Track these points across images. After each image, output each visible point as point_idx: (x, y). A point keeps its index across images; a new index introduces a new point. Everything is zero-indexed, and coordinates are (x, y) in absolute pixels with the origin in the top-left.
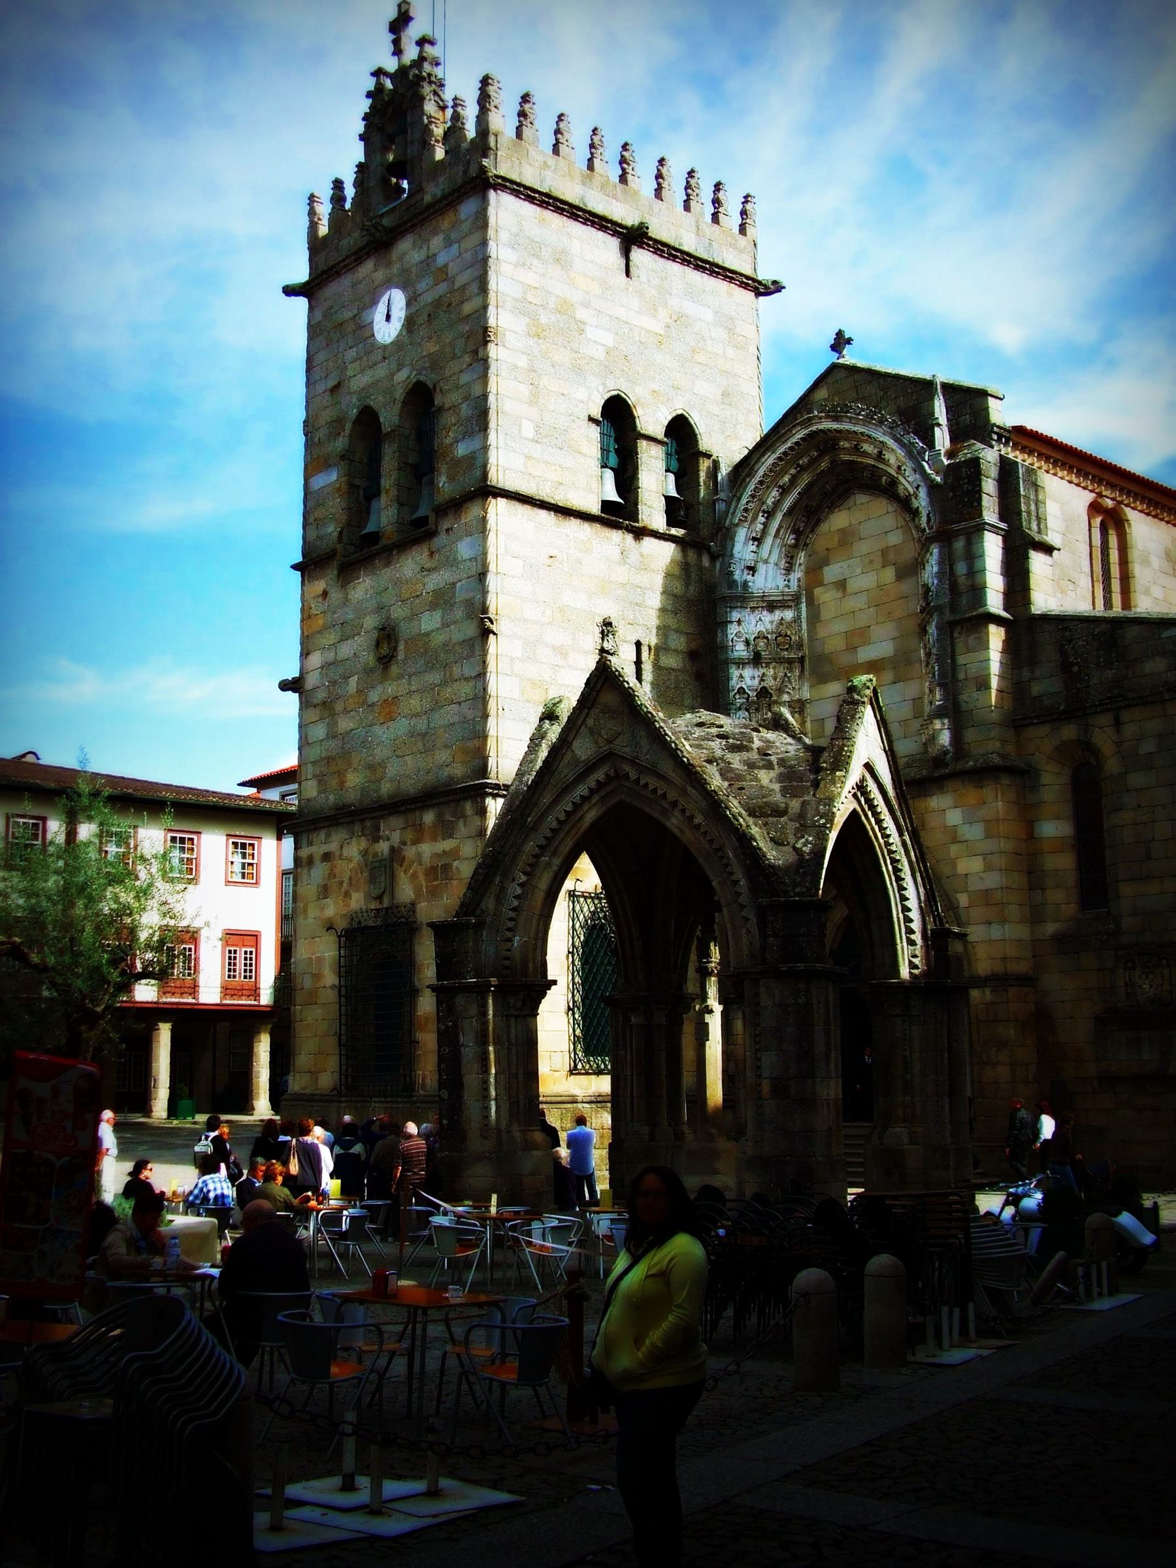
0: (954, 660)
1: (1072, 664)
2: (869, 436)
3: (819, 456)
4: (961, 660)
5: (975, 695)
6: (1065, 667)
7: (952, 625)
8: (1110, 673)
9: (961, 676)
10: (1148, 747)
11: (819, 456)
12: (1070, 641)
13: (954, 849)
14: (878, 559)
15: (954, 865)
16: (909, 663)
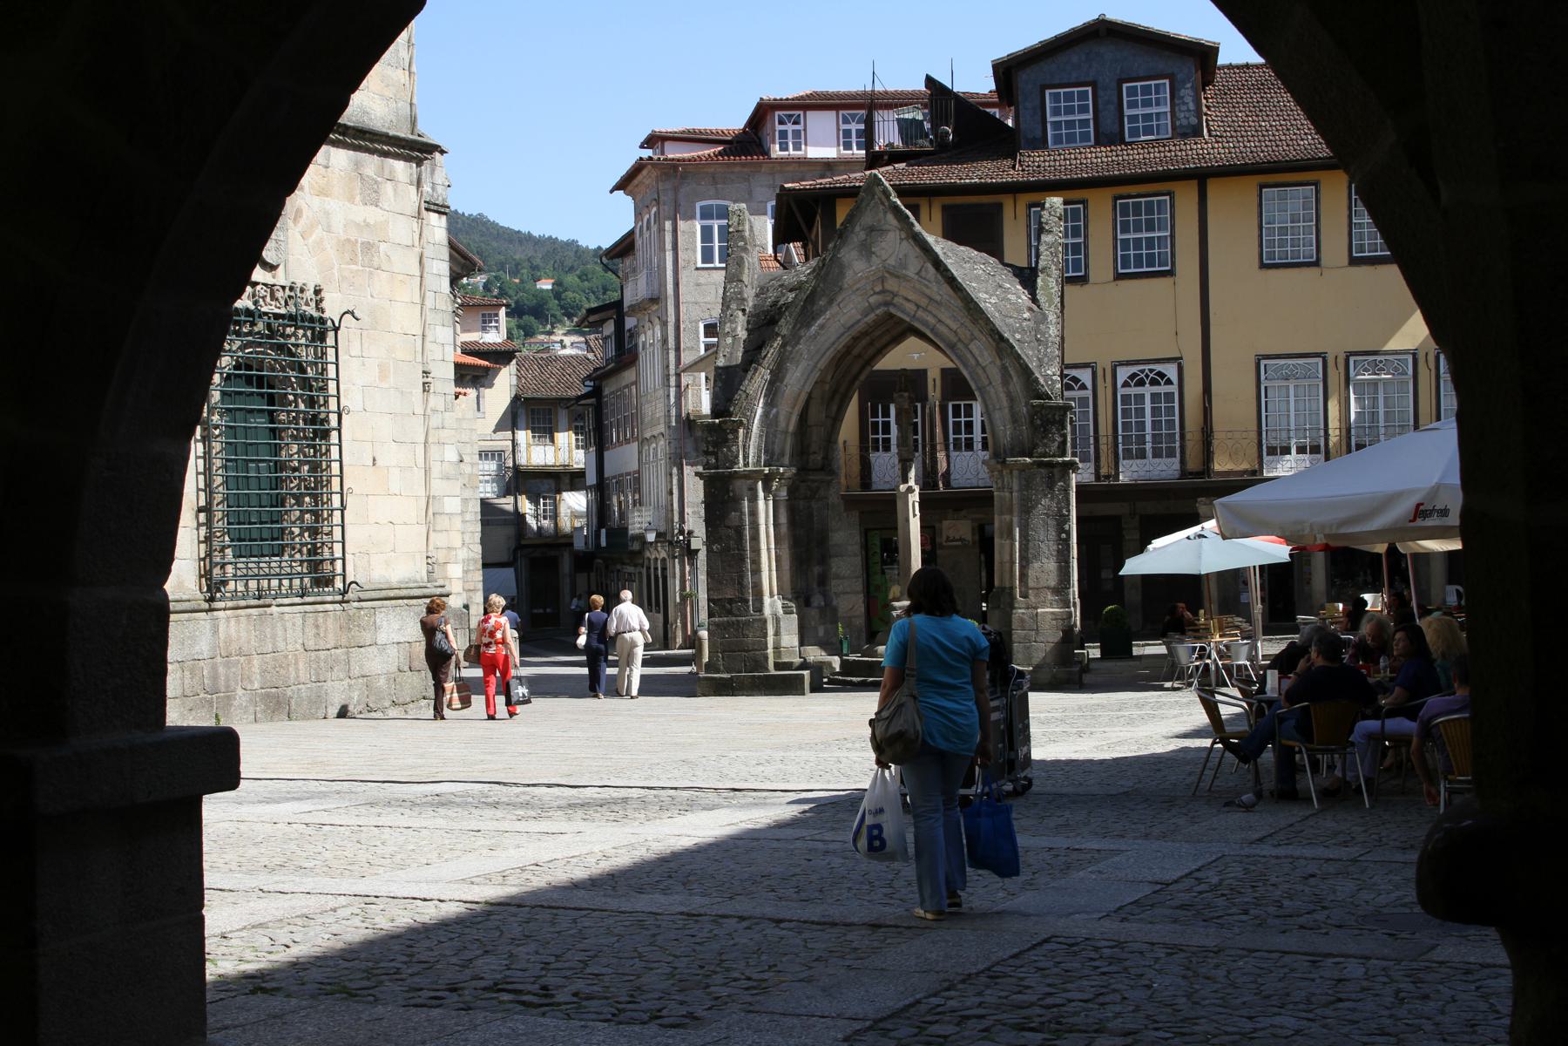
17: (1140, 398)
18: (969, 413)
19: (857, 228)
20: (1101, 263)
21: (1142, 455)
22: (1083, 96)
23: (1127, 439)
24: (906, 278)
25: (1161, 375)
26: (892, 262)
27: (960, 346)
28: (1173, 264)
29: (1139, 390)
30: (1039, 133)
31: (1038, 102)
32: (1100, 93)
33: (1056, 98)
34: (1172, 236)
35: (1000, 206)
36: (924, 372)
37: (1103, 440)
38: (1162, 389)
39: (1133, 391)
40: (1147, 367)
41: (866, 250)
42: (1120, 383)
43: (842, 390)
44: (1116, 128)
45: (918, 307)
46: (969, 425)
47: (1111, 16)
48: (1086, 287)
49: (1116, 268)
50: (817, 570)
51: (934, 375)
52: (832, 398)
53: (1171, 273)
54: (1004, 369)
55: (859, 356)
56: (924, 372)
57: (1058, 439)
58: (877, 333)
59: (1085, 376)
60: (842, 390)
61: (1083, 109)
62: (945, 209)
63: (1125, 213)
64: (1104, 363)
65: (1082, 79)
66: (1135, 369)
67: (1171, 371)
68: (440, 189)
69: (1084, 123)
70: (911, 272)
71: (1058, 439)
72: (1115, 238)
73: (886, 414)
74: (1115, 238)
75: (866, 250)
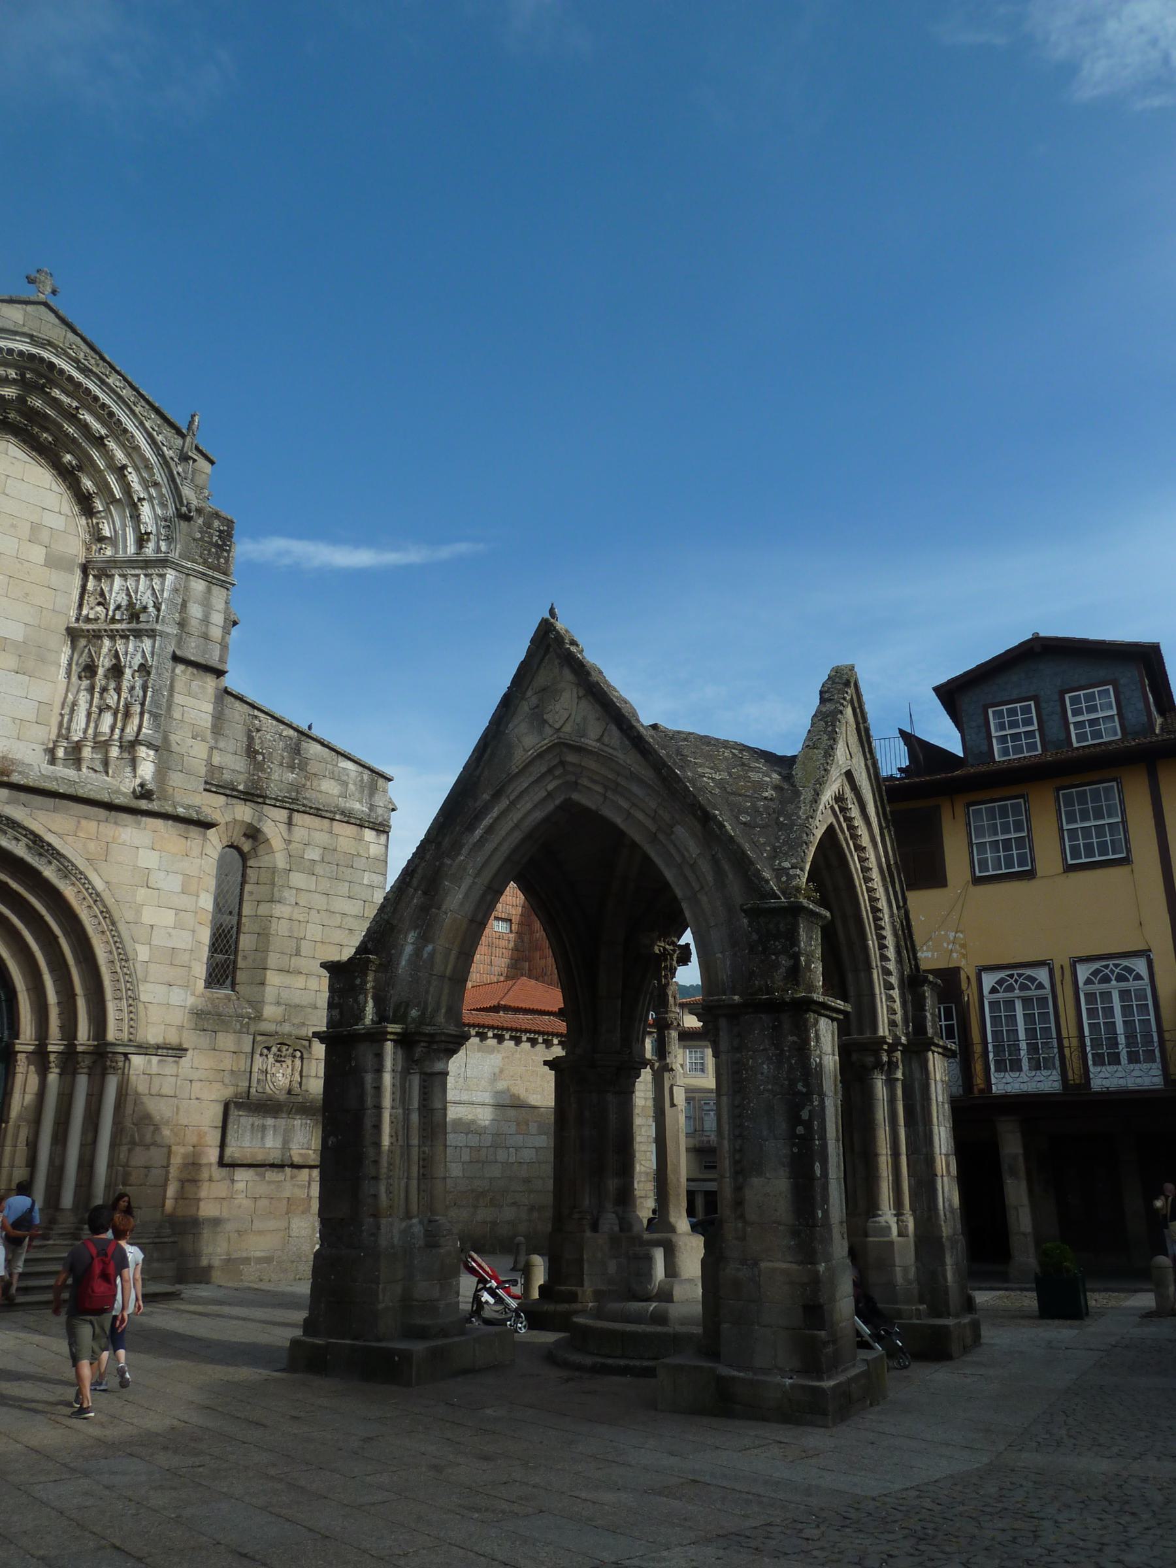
0: (171, 695)
1: (257, 752)
2: (111, 414)
3: (14, 381)
4: (178, 699)
5: (190, 741)
6: (251, 752)
7: (176, 659)
8: (291, 776)
9: (177, 715)
10: (313, 854)
11: (14, 382)
12: (258, 731)
13: (142, 892)
14: (25, 530)
15: (138, 912)
16: (42, 660)
17: (1106, 996)
19: (529, 693)
20: (1048, 856)
21: (1115, 1060)
22: (1027, 710)
23: (1096, 1043)
24: (579, 750)
25: (1129, 970)
26: (567, 728)
27: (661, 837)
28: (1129, 851)
29: (1104, 987)
30: (985, 748)
32: (1044, 705)
33: (999, 715)
34: (1124, 822)
37: (1066, 1043)
38: (1132, 985)
39: (1097, 987)
40: (1111, 963)
41: (538, 720)
42: (1081, 980)
44: (1063, 736)
45: (606, 788)
47: (1042, 635)
48: (1034, 883)
49: (1065, 859)
50: (612, 1184)
53: (1126, 861)
54: (715, 862)
57: (785, 962)
59: (1042, 975)
61: (1028, 722)
63: (1069, 802)
64: (1061, 959)
65: (1024, 695)
67: (1140, 966)
68: (380, 811)
69: (1030, 734)
70: (590, 742)
71: (785, 962)
72: (1061, 829)
74: (1061, 829)
75: (538, 720)
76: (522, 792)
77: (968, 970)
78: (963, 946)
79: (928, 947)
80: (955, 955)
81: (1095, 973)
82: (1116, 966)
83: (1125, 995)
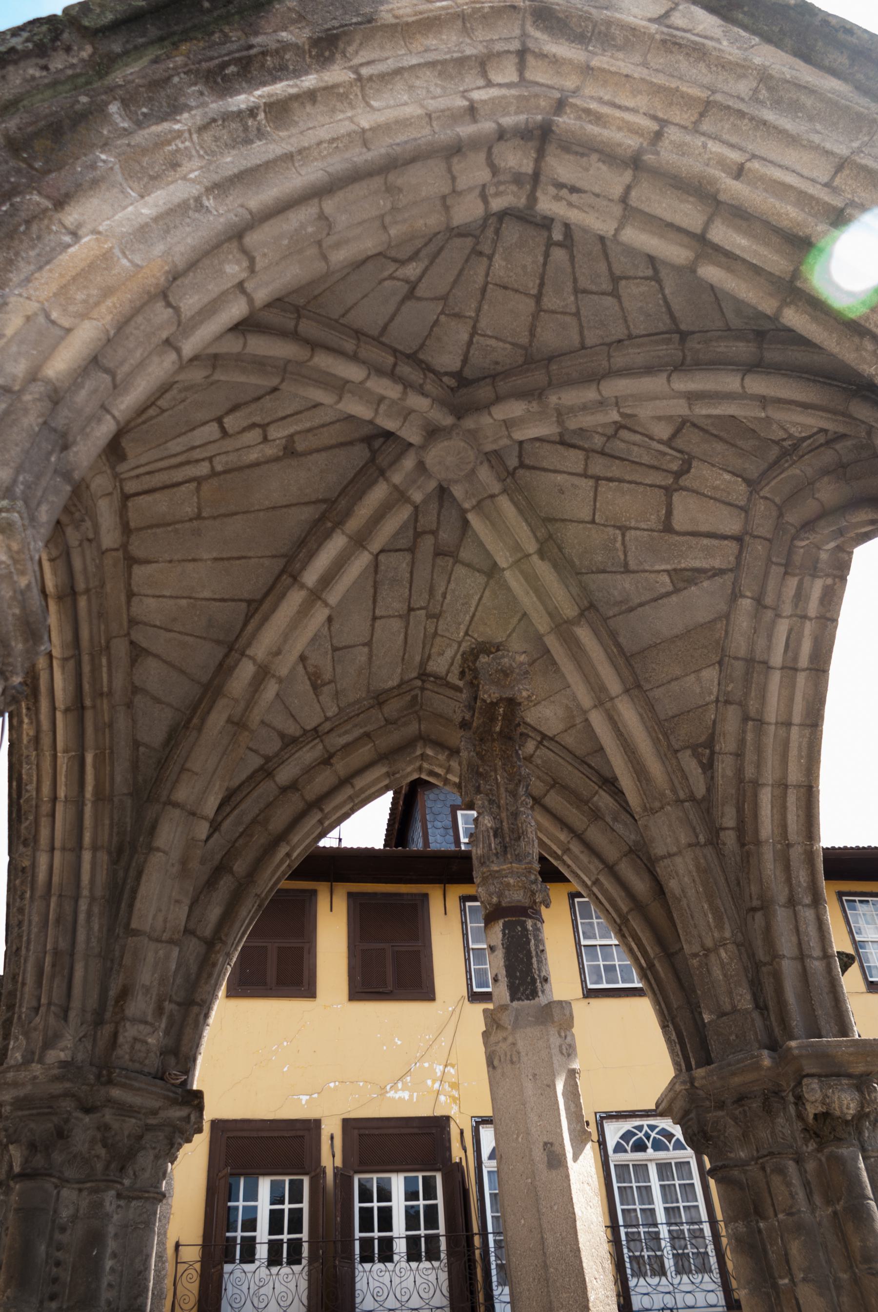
17: (641, 1169)
18: (385, 1195)
29: (639, 1156)
31: (448, 822)
35: (425, 896)
36: (317, 1123)
39: (631, 1157)
40: (645, 1122)
42: (611, 1145)
43: (240, 867)
46: (386, 1217)
49: (583, 981)
51: (331, 1128)
52: (211, 883)
55: (293, 786)
56: (317, 1123)
58: (338, 740)
60: (240, 867)
62: (350, 895)
66: (628, 1125)
72: (578, 944)
73: (252, 1194)
76: (398, 72)
77: (461, 1123)
78: (455, 1086)
79: (405, 1085)
80: (442, 1098)
81: (627, 1136)
82: (652, 1128)
83: (664, 1169)
